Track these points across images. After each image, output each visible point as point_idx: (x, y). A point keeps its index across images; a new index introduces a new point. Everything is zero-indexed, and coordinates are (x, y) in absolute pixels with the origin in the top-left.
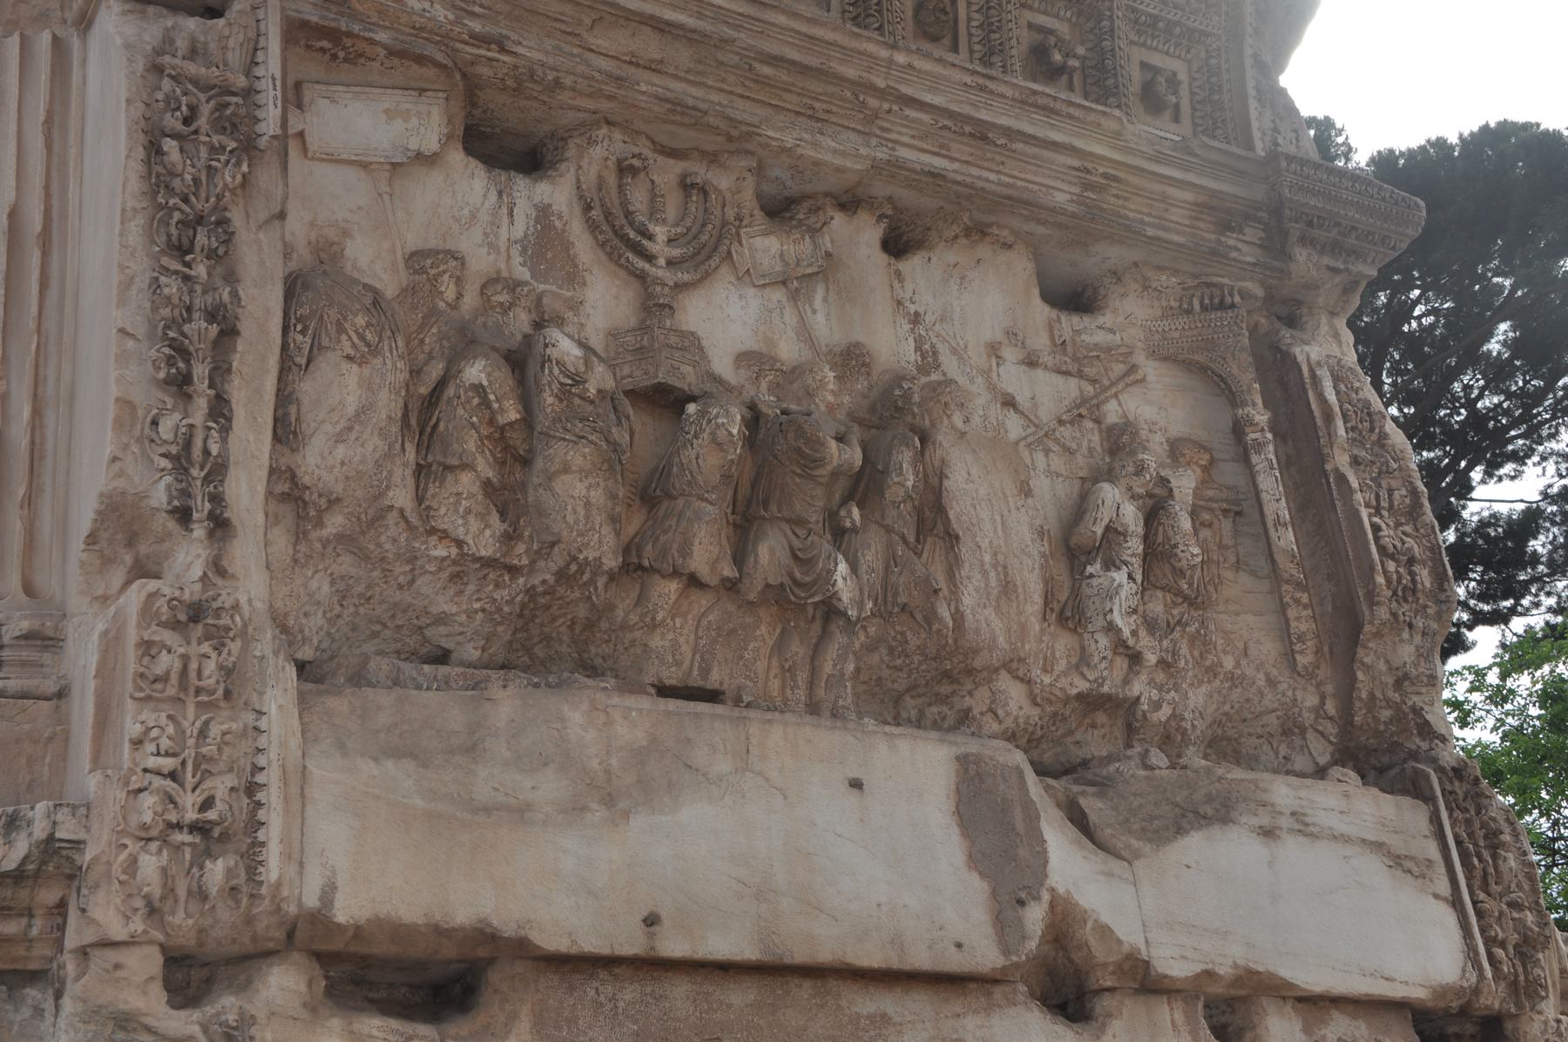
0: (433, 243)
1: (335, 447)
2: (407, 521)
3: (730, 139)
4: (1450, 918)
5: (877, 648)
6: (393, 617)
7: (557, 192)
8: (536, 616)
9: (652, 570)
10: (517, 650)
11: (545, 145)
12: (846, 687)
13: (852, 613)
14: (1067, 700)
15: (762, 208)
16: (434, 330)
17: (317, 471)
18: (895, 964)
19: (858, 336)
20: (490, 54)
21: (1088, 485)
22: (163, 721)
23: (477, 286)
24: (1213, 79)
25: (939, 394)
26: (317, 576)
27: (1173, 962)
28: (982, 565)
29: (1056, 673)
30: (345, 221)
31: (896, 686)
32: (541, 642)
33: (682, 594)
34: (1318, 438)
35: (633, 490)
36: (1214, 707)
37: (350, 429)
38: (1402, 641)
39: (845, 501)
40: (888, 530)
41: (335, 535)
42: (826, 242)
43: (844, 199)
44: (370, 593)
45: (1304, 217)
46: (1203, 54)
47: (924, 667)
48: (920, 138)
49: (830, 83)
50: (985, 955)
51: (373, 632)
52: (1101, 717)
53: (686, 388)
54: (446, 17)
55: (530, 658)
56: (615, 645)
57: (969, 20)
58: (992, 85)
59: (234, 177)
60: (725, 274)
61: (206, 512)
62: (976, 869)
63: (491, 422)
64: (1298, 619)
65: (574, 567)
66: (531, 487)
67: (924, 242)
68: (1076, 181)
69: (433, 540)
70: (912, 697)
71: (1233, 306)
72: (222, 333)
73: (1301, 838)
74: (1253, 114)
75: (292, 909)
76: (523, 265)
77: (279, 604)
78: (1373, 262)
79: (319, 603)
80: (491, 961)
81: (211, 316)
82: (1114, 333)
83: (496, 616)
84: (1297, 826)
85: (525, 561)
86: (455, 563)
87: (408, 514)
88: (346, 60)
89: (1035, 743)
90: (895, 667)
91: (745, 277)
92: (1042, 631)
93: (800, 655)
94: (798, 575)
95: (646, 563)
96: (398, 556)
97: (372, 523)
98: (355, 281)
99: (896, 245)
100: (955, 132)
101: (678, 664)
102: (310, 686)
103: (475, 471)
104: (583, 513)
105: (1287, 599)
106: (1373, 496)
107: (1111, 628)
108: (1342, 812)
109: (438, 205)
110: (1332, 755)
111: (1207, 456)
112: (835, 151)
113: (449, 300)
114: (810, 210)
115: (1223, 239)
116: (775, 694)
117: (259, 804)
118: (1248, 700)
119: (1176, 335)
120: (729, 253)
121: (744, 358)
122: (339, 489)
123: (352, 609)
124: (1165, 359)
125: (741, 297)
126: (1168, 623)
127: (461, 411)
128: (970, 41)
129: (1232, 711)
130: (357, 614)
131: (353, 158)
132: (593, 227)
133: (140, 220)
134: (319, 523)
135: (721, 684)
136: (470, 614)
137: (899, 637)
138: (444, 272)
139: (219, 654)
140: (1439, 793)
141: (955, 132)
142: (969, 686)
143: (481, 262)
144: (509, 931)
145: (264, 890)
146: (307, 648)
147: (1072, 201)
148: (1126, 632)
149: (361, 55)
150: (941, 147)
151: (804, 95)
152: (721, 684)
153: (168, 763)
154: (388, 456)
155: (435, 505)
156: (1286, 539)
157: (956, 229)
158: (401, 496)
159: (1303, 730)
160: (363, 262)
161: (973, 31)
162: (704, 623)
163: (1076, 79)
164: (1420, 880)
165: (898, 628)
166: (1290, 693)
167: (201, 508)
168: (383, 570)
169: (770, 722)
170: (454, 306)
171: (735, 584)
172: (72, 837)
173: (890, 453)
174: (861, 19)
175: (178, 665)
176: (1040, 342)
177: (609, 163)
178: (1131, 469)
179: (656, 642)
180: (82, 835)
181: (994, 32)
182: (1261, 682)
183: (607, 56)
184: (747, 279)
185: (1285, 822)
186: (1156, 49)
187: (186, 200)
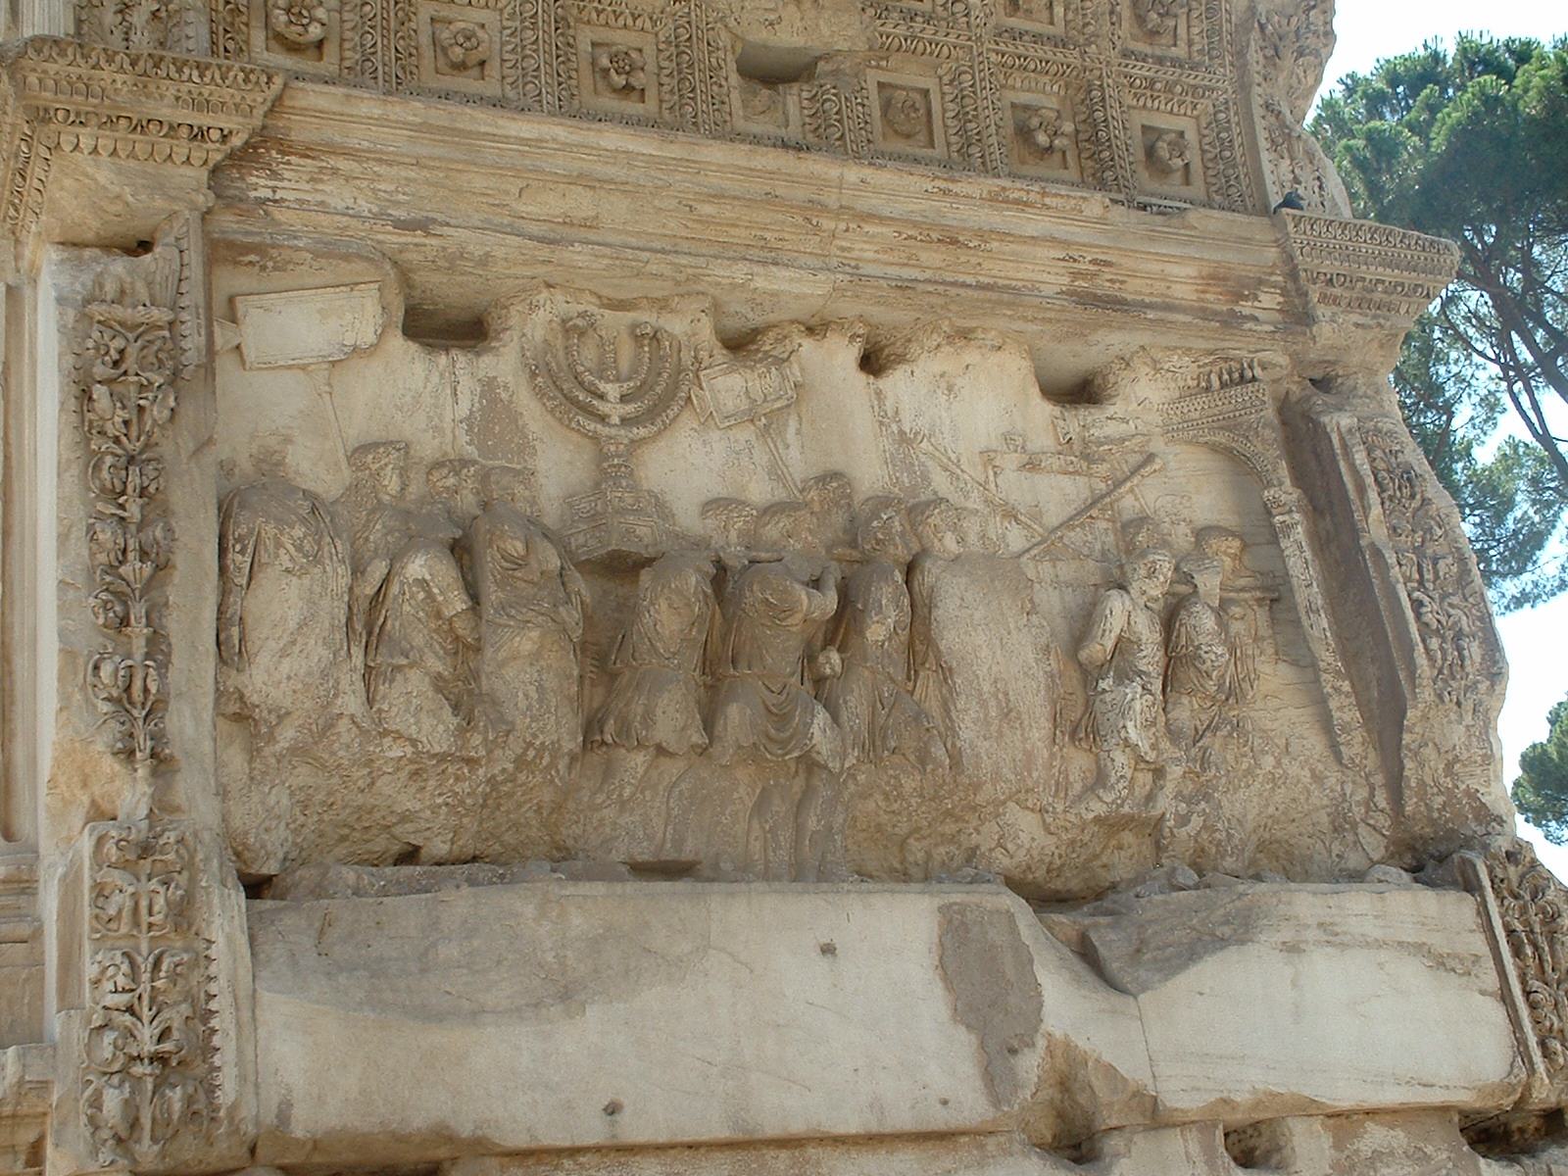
0: (376, 435)
1: (280, 662)
3: (678, 283)
4: (1497, 1013)
7: (502, 363)
8: (499, 805)
10: (487, 839)
13: (834, 765)
16: (378, 527)
18: (874, 1128)
19: (837, 462)
20: (416, 240)
22: (118, 959)
24: (1224, 135)
26: (274, 791)
27: (1180, 1094)
34: (1352, 512)
36: (1256, 811)
37: (294, 643)
38: (1450, 722)
39: (824, 648)
42: (794, 371)
43: (813, 322)
45: (1322, 277)
46: (1211, 110)
50: (971, 1105)
52: (1127, 837)
54: (370, 211)
55: (502, 845)
57: (944, 111)
58: (956, 188)
59: (160, 412)
60: (688, 422)
61: (148, 751)
62: (962, 1022)
63: (438, 615)
64: (1341, 709)
65: (531, 753)
66: (483, 678)
68: (1063, 271)
69: (387, 741)
70: (917, 840)
71: (1254, 379)
72: (158, 568)
73: (1329, 950)
74: (1267, 167)
75: (251, 1130)
77: (236, 824)
80: (454, 1160)
84: (1326, 938)
86: (411, 761)
88: (275, 269)
91: (707, 420)
92: (1052, 755)
95: (610, 741)
98: (294, 489)
99: (872, 362)
105: (1328, 689)
106: (1415, 568)
107: (1126, 742)
108: (1376, 917)
110: (1387, 848)
113: (393, 492)
114: (777, 339)
117: (214, 1031)
118: (1294, 800)
119: (1197, 415)
122: (287, 703)
123: (316, 818)
126: (1196, 729)
127: (406, 608)
129: (1277, 813)
130: (321, 821)
132: (540, 393)
133: (75, 470)
134: (271, 738)
135: (697, 854)
136: (435, 809)
140: (1486, 883)
143: (428, 447)
144: (466, 1131)
145: (222, 1113)
148: (1144, 746)
151: (752, 228)
153: (122, 999)
154: (334, 663)
155: (385, 707)
156: (1320, 627)
157: (936, 339)
158: (352, 702)
159: (1354, 826)
160: (305, 466)
161: (949, 122)
162: (677, 791)
164: (1465, 978)
165: (891, 772)
166: (1339, 788)
167: (144, 744)
168: (341, 777)
169: (732, 894)
171: (706, 749)
172: (41, 1078)
174: (822, 130)
175: (129, 904)
176: (1042, 440)
177: (554, 325)
178: (1143, 572)
179: (626, 819)
180: (50, 1077)
185: (1312, 934)
187: (117, 440)
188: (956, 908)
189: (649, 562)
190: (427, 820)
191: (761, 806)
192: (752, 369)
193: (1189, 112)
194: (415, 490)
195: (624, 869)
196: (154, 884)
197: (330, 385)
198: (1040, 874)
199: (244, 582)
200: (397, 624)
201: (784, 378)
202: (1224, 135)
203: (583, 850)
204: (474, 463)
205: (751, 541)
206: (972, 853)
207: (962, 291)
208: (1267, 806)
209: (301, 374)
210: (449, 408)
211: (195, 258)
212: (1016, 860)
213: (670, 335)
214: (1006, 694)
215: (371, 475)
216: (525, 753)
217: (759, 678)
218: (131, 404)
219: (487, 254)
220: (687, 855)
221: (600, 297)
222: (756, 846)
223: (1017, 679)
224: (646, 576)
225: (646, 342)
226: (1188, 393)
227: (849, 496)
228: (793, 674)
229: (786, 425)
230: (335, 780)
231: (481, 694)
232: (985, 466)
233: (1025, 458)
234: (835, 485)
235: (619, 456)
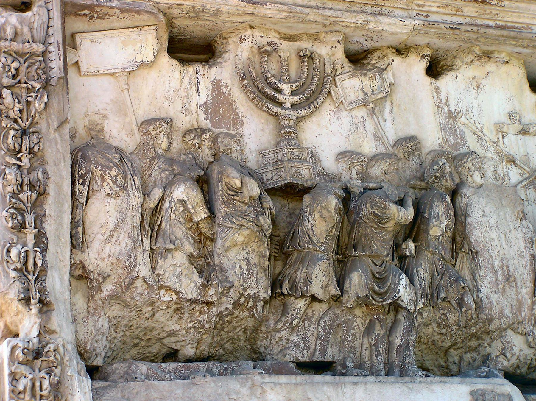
0: (152, 116)
1: (104, 247)
2: (147, 284)
3: (325, 26)
5: (430, 324)
6: (145, 334)
8: (224, 328)
9: (289, 295)
12: (410, 351)
13: (411, 308)
16: (156, 168)
17: (96, 261)
19: (412, 131)
25: (465, 163)
26: (101, 319)
28: (493, 267)
31: (444, 344)
32: (228, 341)
33: (308, 307)
35: (278, 247)
37: (112, 236)
39: (405, 240)
41: (108, 296)
42: (389, 76)
44: (131, 324)
47: (460, 332)
48: (443, 7)
51: (135, 344)
53: (305, 184)
55: (224, 350)
56: (271, 340)
60: (328, 107)
61: (37, 299)
63: (191, 220)
65: (243, 300)
69: (162, 292)
70: (455, 349)
72: (39, 195)
77: (81, 338)
79: (103, 333)
81: (32, 187)
85: (215, 299)
86: (176, 303)
88: (98, 18)
89: (532, 370)
90: (442, 334)
93: (381, 336)
94: (377, 288)
95: (286, 292)
96: (144, 304)
97: (128, 287)
98: (110, 147)
101: (308, 348)
102: (101, 384)
104: (246, 267)
109: (155, 91)
112: (390, 24)
113: (164, 148)
114: (379, 57)
116: (366, 359)
120: (329, 93)
121: (342, 155)
122: (108, 270)
127: (173, 216)
132: (246, 90)
135: (333, 357)
136: (187, 330)
137: (442, 317)
138: (160, 132)
139: (50, 376)
142: (488, 340)
146: (99, 358)
149: (106, 15)
150: (457, 11)
152: (333, 357)
154: (134, 248)
157: (471, 57)
162: (322, 322)
165: (442, 311)
168: (137, 311)
169: (356, 383)
171: (339, 298)
173: (431, 207)
179: (294, 337)
184: (341, 106)
188: (480, 392)
189: (307, 190)
191: (369, 330)
192: (365, 74)
194: (177, 145)
195: (292, 365)
196: (43, 374)
197: (128, 85)
198: (524, 370)
199: (84, 201)
200: (168, 225)
201: (383, 80)
203: (270, 354)
204: (209, 130)
205: (363, 176)
206: (486, 359)
207: (487, 30)
209: (112, 79)
210: (194, 99)
211: (56, 14)
212: (511, 363)
213: (319, 55)
214: (508, 267)
215: (152, 138)
216: (240, 298)
218: (23, 100)
219: (217, 10)
220: (328, 358)
222: (366, 354)
223: (514, 258)
224: (307, 198)
225: (306, 59)
227: (420, 150)
228: (388, 255)
229: (384, 108)
231: (214, 265)
232: (497, 132)
233: (520, 127)
234: (412, 143)
235: (291, 127)
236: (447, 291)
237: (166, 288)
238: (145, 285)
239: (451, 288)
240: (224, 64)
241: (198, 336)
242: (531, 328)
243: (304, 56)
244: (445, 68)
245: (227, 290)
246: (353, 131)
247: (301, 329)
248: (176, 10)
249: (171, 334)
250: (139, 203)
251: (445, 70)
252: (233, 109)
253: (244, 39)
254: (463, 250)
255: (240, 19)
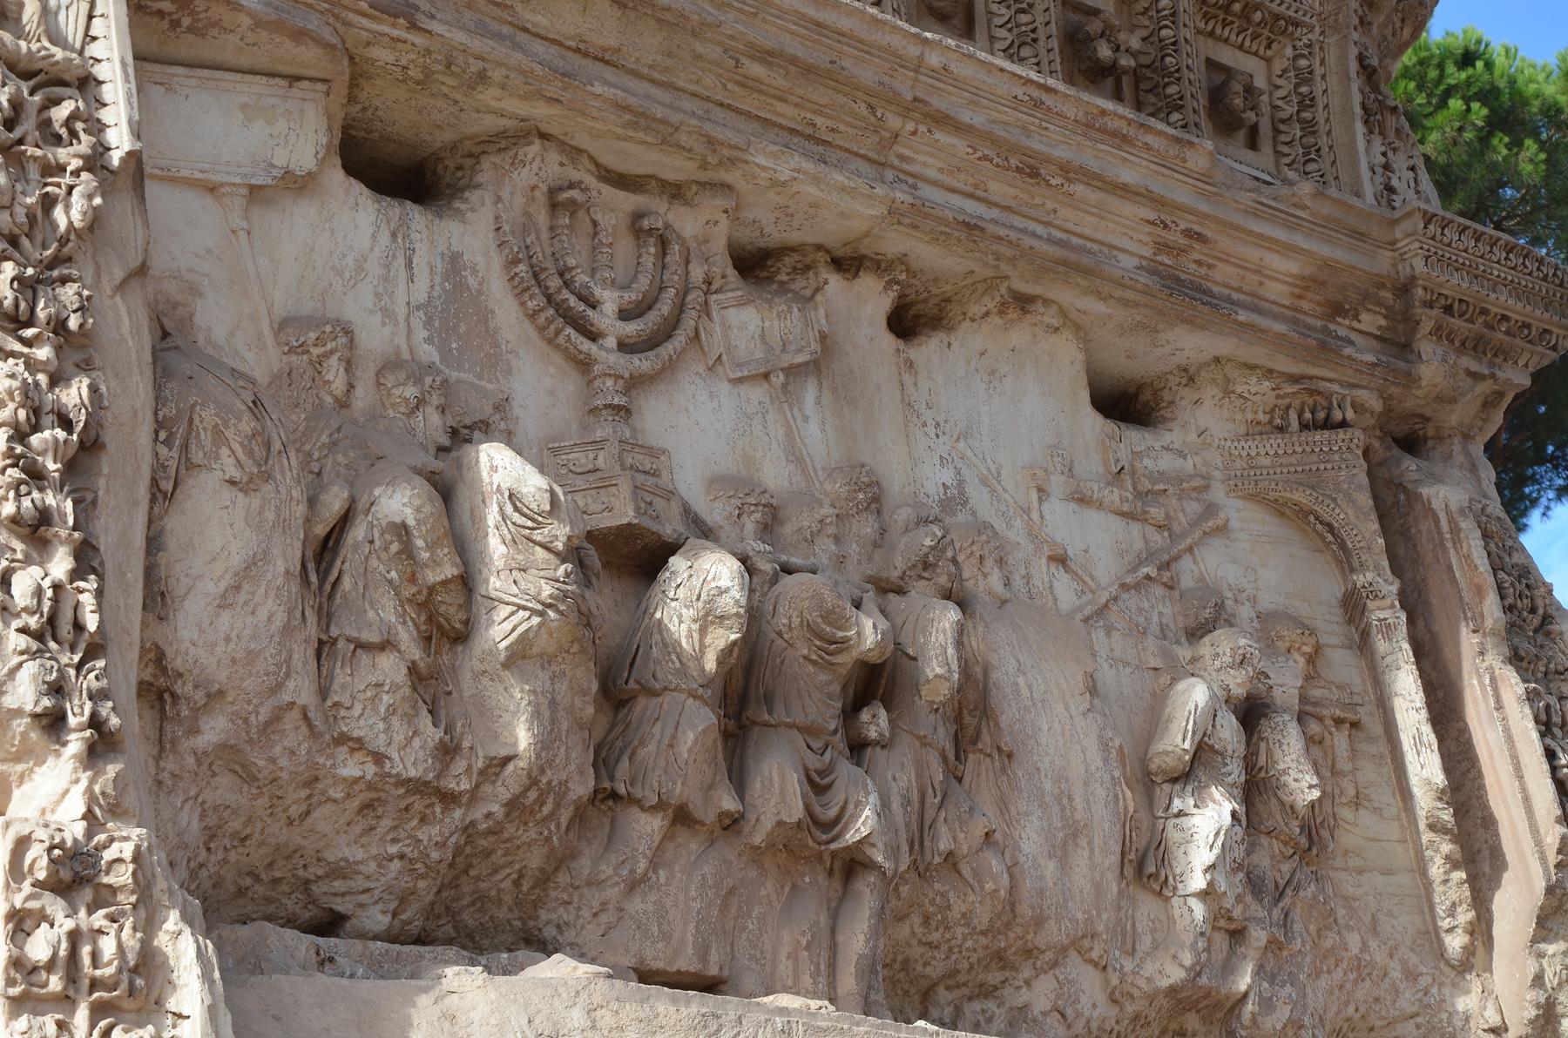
1: (217, 615)
2: (310, 725)
5: (906, 916)
6: (270, 865)
8: (470, 866)
9: (632, 800)
10: (439, 917)
11: (441, 160)
14: (1151, 998)
15: (736, 267)
20: (395, 33)
21: (1165, 679)
23: (371, 373)
24: (1304, 89)
26: (188, 806)
29: (1139, 954)
30: (191, 270)
31: (928, 970)
33: (668, 836)
36: (1334, 1009)
37: (238, 588)
40: (924, 741)
43: (840, 253)
44: (248, 831)
46: (1289, 52)
47: (969, 944)
49: (838, 92)
56: (579, 909)
61: (86, 718)
63: (413, 580)
67: (941, 319)
68: (1146, 239)
70: (948, 988)
76: (429, 340)
78: (1526, 365)
82: (1185, 458)
83: (418, 865)
85: (465, 785)
86: (370, 786)
87: (311, 715)
88: (190, 30)
90: (929, 944)
95: (622, 790)
100: (998, 165)
103: (399, 652)
104: (547, 714)
111: (1313, 641)
113: (339, 393)
114: (795, 269)
115: (1332, 327)
118: (1377, 1000)
119: (1267, 462)
121: (719, 483)
122: (222, 675)
124: (1251, 497)
125: (711, 395)
127: (374, 562)
128: (989, 22)
130: (225, 861)
131: (198, 175)
135: (721, 969)
137: (938, 899)
138: (332, 352)
139: (121, 929)
141: (998, 165)
142: (1027, 972)
147: (1140, 268)
149: (214, 25)
154: (287, 630)
157: (989, 303)
163: (1126, 82)
168: (271, 798)
170: (343, 404)
171: (735, 821)
176: (1091, 466)
177: (537, 193)
178: (1227, 659)
179: (636, 905)
181: (1023, 11)
182: (1396, 974)
183: (545, 39)
186: (1226, 40)
190: (368, 877)
192: (769, 302)
193: (1261, 52)
202: (1304, 89)
204: (439, 372)
207: (1036, 243)
208: (1347, 1004)
209: (209, 200)
210: (402, 286)
213: (679, 237)
214: (1070, 799)
217: (800, 729)
221: (597, 165)
226: (1256, 430)
230: (263, 802)
236: (954, 838)
237: (350, 744)
238: (304, 729)
239: (962, 831)
240: (469, 215)
241: (406, 882)
242: (1117, 953)
243: (651, 229)
244: (923, 320)
245: (496, 766)
246: (742, 430)
247: (651, 888)
248: (385, 52)
249: (339, 871)
250: (298, 515)
251: (925, 325)
252: (487, 330)
253: (522, 161)
254: (980, 746)
255: (520, 108)
